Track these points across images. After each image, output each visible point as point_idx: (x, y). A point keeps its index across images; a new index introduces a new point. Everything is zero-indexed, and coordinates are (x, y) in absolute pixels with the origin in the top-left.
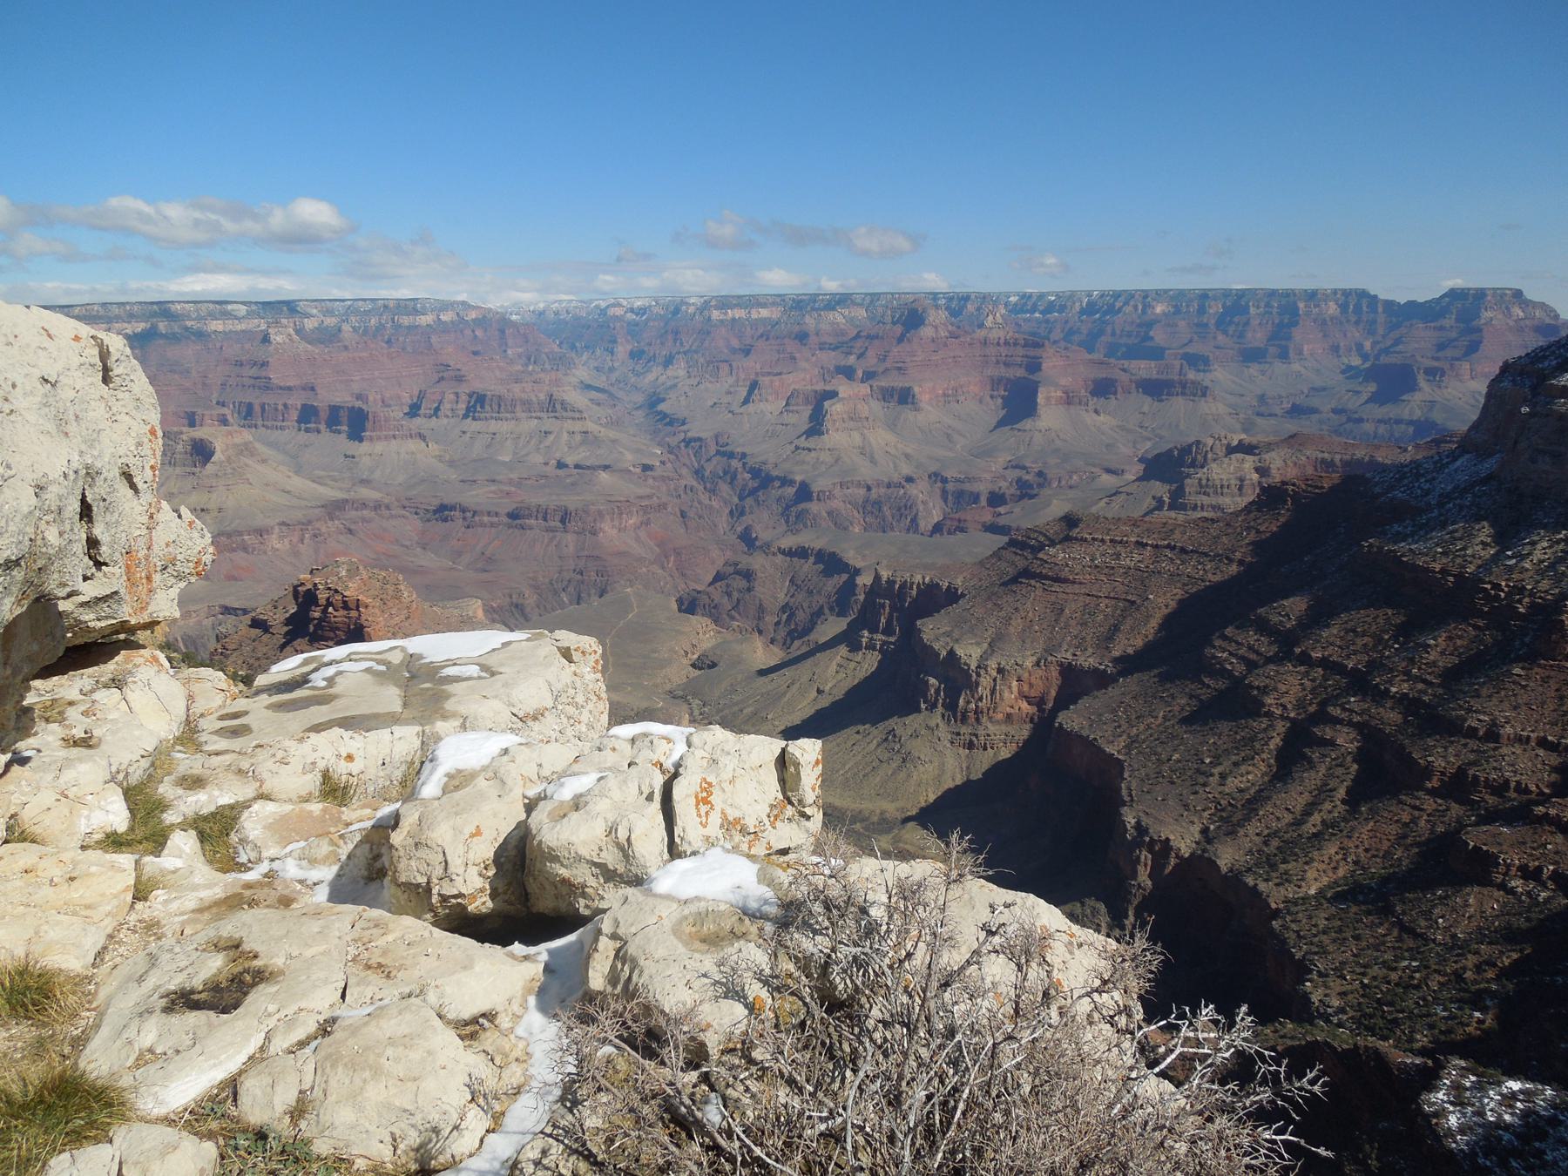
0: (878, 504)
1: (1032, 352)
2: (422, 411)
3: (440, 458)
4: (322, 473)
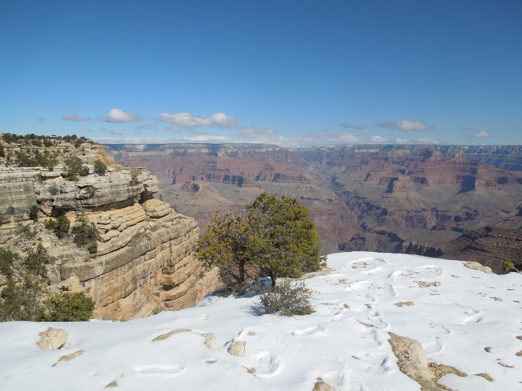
0: (411, 218)
1: (473, 167)
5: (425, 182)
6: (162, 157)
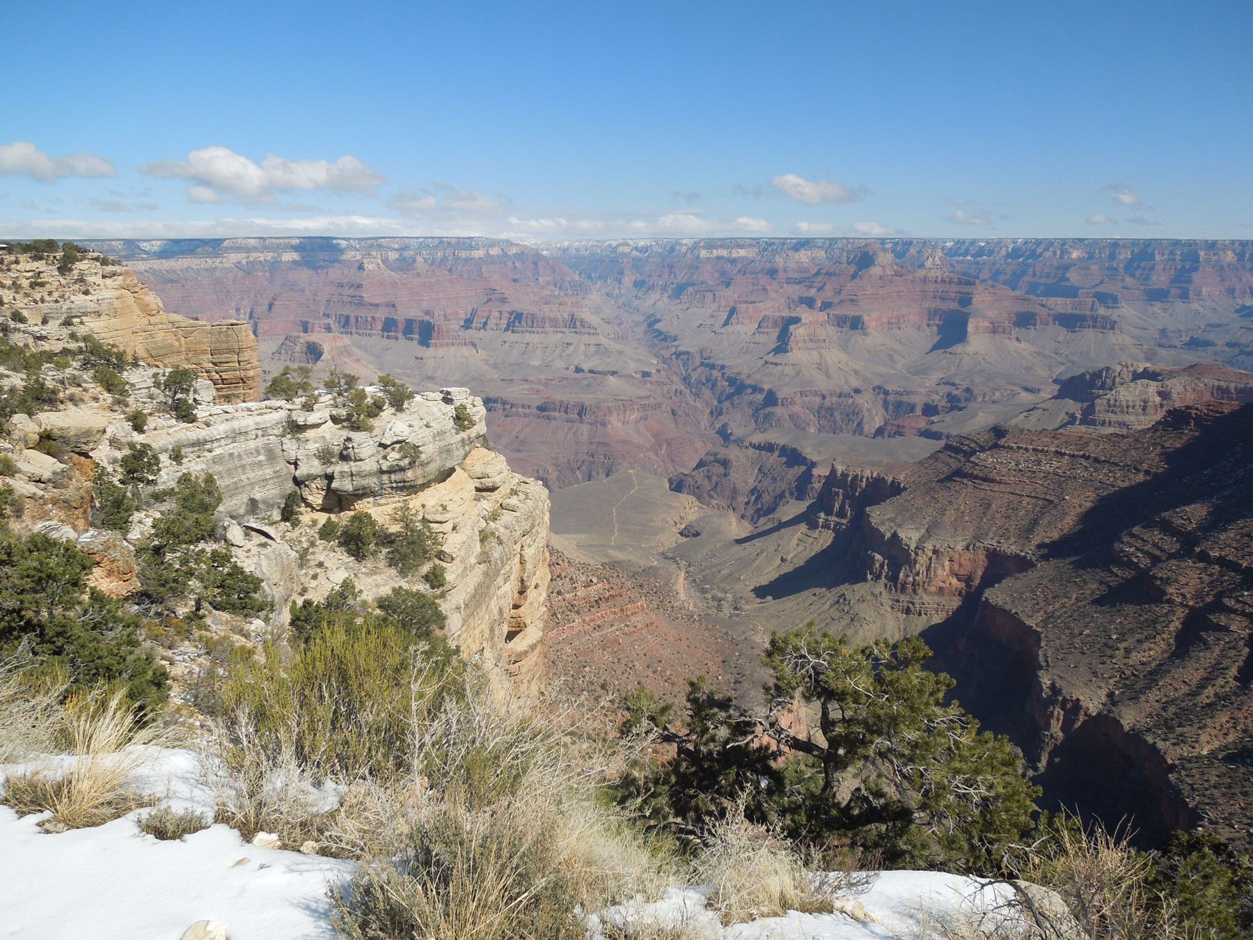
0: (830, 410)
1: (965, 289)
3: (486, 362)
6: (218, 274)
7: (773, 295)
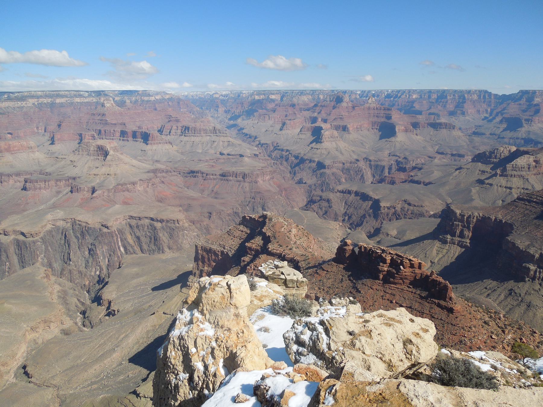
0: (348, 170)
1: (387, 112)
2: (164, 133)
3: (177, 151)
4: (141, 158)
5: (346, 130)
6: (24, 110)
7: (298, 116)
